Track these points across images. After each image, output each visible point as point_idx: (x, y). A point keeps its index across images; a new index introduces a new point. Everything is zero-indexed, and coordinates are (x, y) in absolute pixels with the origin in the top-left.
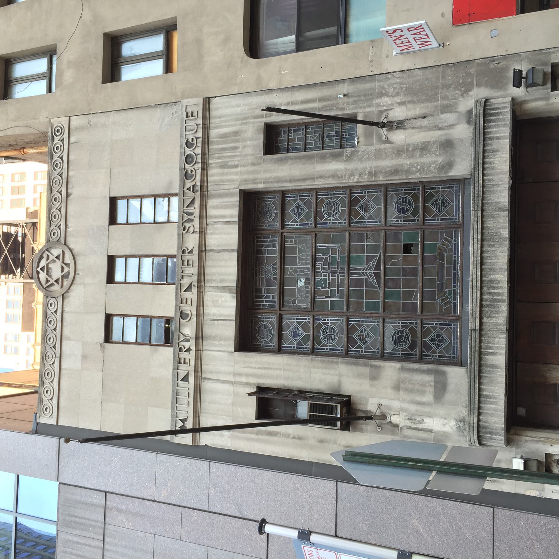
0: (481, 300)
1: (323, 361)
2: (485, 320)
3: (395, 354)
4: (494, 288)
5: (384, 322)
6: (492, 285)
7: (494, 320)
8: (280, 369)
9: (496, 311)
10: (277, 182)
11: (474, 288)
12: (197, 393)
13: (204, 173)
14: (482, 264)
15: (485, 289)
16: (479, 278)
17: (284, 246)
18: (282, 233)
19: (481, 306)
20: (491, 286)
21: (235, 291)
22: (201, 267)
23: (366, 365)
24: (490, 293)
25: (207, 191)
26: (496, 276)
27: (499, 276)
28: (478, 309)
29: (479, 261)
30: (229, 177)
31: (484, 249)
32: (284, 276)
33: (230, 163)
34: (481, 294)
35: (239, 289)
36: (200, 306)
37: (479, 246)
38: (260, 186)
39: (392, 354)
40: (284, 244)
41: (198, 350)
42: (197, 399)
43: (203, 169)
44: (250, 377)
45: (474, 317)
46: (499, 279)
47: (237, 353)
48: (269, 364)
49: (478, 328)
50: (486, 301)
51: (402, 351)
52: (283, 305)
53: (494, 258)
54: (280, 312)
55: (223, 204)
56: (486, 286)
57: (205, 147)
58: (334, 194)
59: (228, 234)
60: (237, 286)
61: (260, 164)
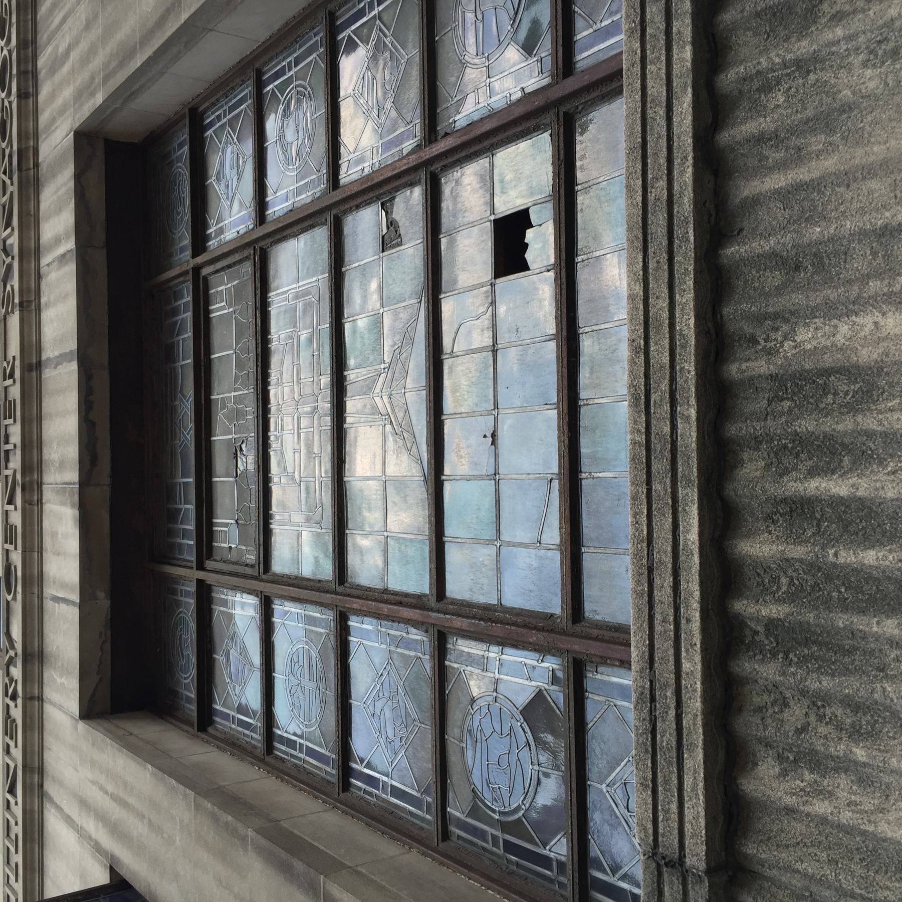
0: (724, 576)
1: (215, 819)
2: (766, 781)
3: (482, 835)
4: (830, 454)
5: (441, 651)
6: (807, 425)
7: (840, 803)
8: (141, 816)
9: (855, 706)
10: (121, 65)
11: (660, 466)
12: (33, 840)
13: (27, 105)
14: (718, 220)
15: (751, 470)
16: (689, 367)
17: (208, 320)
18: (197, 270)
19: (725, 638)
20: (803, 444)
21: (76, 498)
22: (31, 421)
23: (312, 888)
24: (799, 512)
25: (37, 165)
26: (844, 329)
27: (866, 321)
28: (693, 664)
29: (686, 205)
30: (59, 101)
31: (729, 78)
32: (209, 433)
33: (61, 49)
34: (722, 519)
35: (102, 492)
36: (32, 550)
37: (684, 55)
38: (99, 99)
39: (474, 831)
40: (207, 312)
41: (32, 698)
42: (33, 861)
43: (23, 95)
44: (100, 824)
45: (666, 738)
46: (867, 355)
47: (81, 725)
48: (125, 784)
49: (697, 856)
50: (766, 592)
51: (505, 827)
52: (210, 548)
53: (817, 142)
54: (201, 575)
55: (55, 197)
56: (757, 441)
57: (26, 21)
58: (297, 62)
59: (66, 297)
60: (85, 482)
61: (96, 17)
